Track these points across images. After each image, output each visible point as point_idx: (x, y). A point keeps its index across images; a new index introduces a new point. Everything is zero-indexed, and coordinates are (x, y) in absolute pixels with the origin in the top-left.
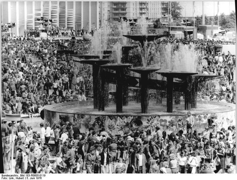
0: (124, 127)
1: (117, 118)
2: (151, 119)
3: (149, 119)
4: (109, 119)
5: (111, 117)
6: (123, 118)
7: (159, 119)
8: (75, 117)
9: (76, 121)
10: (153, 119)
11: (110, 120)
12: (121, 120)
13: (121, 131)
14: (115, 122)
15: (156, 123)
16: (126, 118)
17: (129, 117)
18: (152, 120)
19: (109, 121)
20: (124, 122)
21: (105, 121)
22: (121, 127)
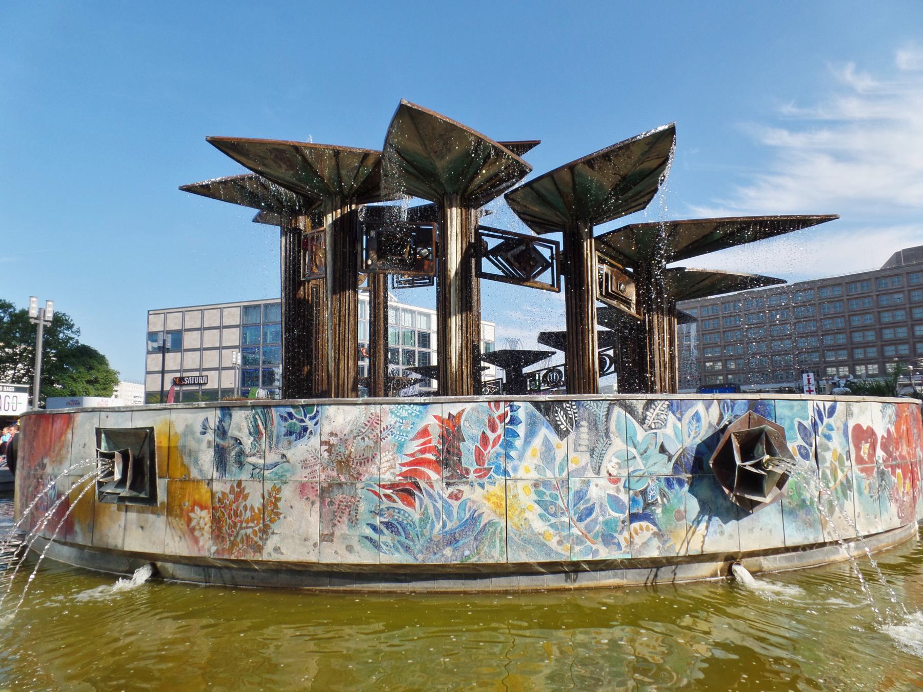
0: (663, 495)
1: (608, 416)
2: (815, 425)
3: (807, 424)
4: (545, 432)
5: (561, 417)
6: (649, 421)
7: (851, 425)
8: (232, 432)
9: (241, 465)
10: (826, 420)
11: (554, 438)
12: (640, 434)
13: (644, 524)
14: (592, 452)
15: (839, 450)
16: (671, 418)
17: (690, 413)
18: (821, 429)
19: (546, 442)
20: (663, 450)
21: (508, 445)
22: (644, 493)
